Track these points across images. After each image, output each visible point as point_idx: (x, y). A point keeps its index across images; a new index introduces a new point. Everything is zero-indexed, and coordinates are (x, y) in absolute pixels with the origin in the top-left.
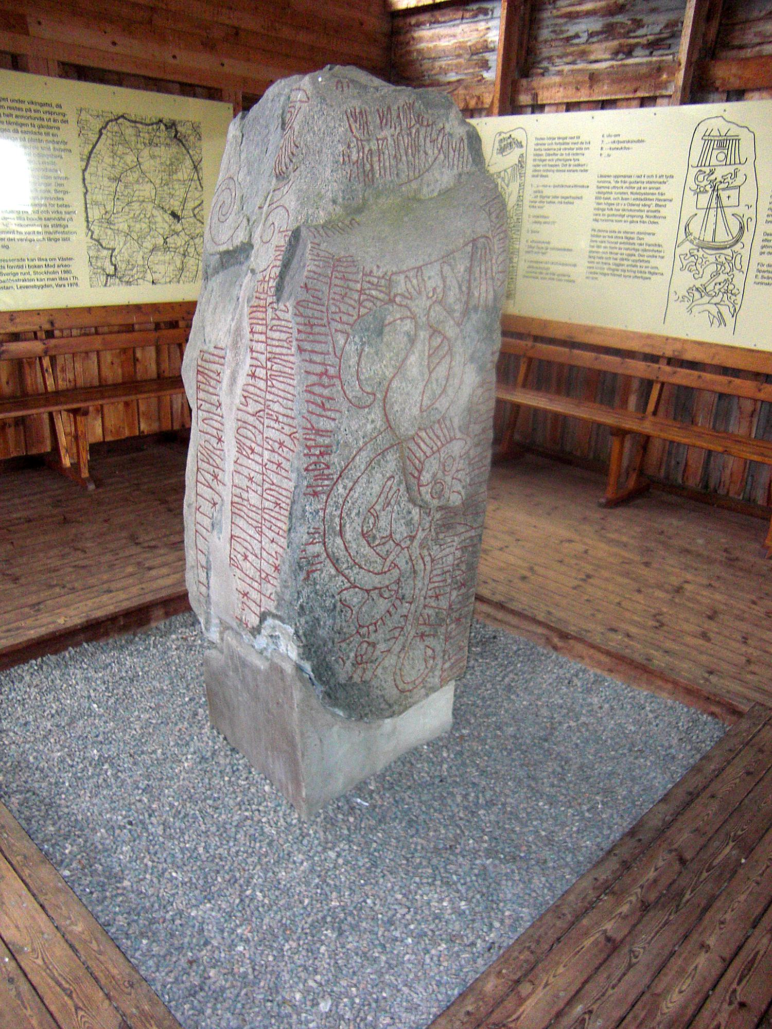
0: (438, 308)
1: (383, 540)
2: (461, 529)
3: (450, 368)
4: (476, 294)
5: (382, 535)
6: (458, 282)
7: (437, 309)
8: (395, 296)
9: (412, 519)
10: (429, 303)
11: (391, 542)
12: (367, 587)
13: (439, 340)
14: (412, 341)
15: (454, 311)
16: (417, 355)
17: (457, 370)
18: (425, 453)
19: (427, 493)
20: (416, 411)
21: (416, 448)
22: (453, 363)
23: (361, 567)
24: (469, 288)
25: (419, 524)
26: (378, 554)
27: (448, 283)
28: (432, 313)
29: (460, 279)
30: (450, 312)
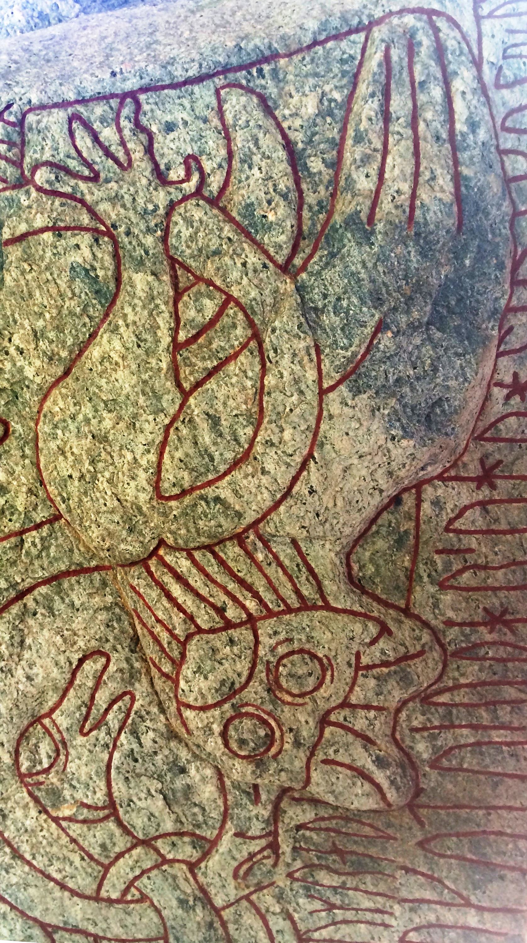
0: (197, 212)
1: (85, 813)
2: (414, 888)
3: (261, 391)
4: (365, 184)
5: (79, 795)
6: (289, 145)
7: (198, 214)
8: (35, 168)
9: (188, 789)
10: (161, 198)
11: (111, 825)
12: (47, 920)
13: (210, 307)
14: (109, 296)
15: (269, 227)
16: (127, 334)
17: (291, 402)
18: (191, 618)
19: (208, 730)
20: (137, 491)
21: (154, 594)
22: (270, 380)
23: (17, 854)
24: (336, 165)
25: (225, 815)
26: (73, 841)
27: (240, 139)
28: (179, 227)
29: (298, 137)
30: (249, 229)
